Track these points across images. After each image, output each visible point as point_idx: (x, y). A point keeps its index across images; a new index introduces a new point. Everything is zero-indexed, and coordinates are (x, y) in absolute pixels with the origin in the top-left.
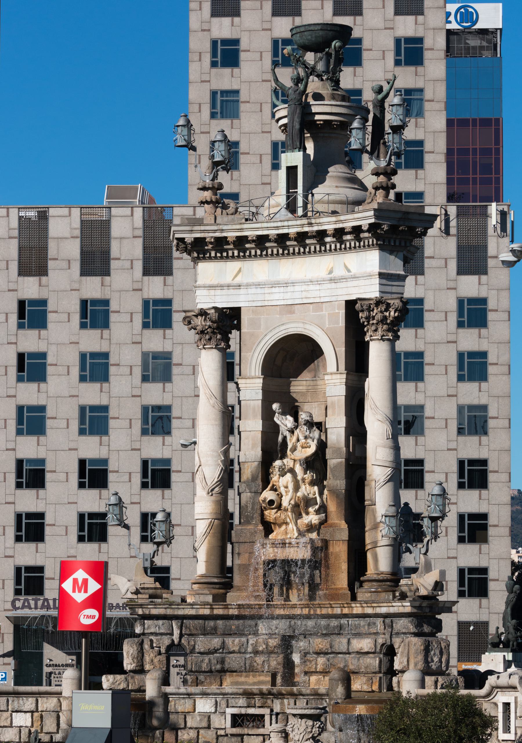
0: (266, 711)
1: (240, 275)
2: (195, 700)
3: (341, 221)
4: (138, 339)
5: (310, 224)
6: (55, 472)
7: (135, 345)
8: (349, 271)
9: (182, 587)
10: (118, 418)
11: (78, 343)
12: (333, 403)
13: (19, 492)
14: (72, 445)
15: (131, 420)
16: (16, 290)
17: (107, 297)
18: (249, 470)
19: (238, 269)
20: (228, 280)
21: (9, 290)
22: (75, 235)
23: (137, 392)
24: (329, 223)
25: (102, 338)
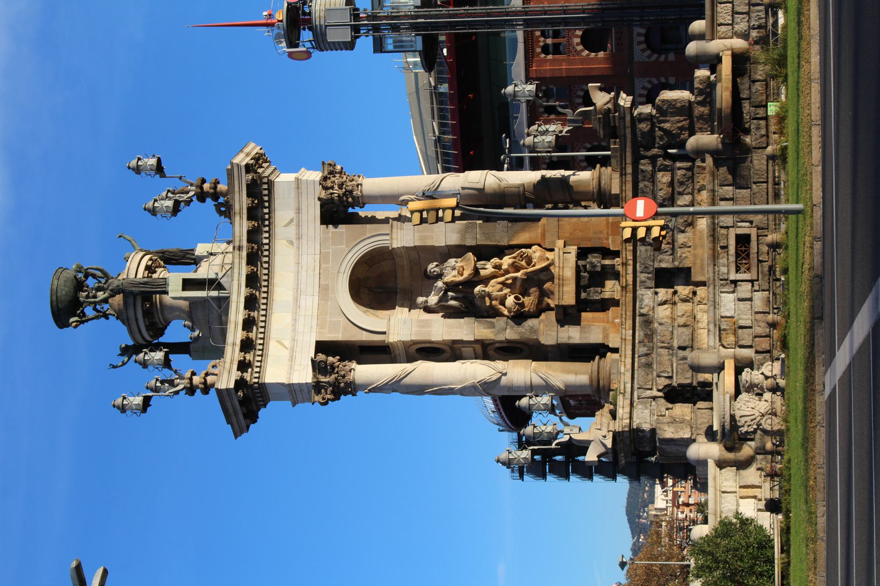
0: (732, 233)
1: (283, 342)
2: (722, 317)
3: (241, 209)
5: (240, 248)
8: (292, 221)
12: (422, 238)
18: (483, 330)
19: (277, 344)
20: (286, 353)
24: (241, 225)
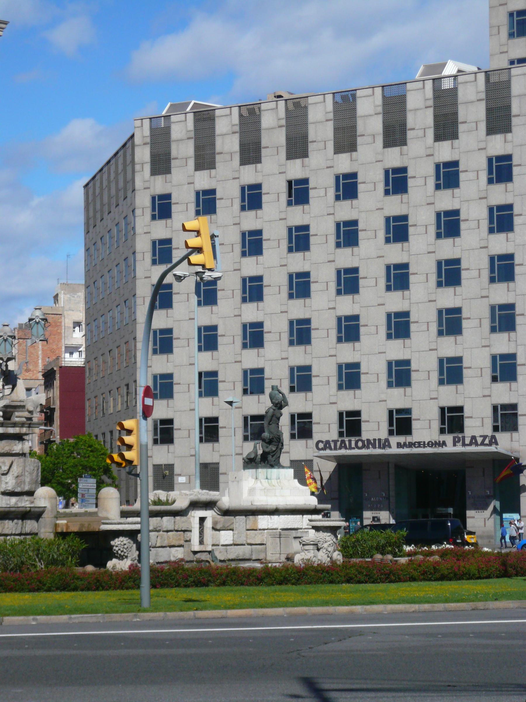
4: (431, 200)
6: (367, 326)
7: (429, 206)
9: (474, 425)
10: (416, 274)
11: (382, 209)
13: (340, 345)
14: (381, 301)
15: (427, 274)
16: (333, 167)
17: (405, 165)
21: (327, 167)
22: (378, 112)
23: (431, 249)
25: (402, 202)
